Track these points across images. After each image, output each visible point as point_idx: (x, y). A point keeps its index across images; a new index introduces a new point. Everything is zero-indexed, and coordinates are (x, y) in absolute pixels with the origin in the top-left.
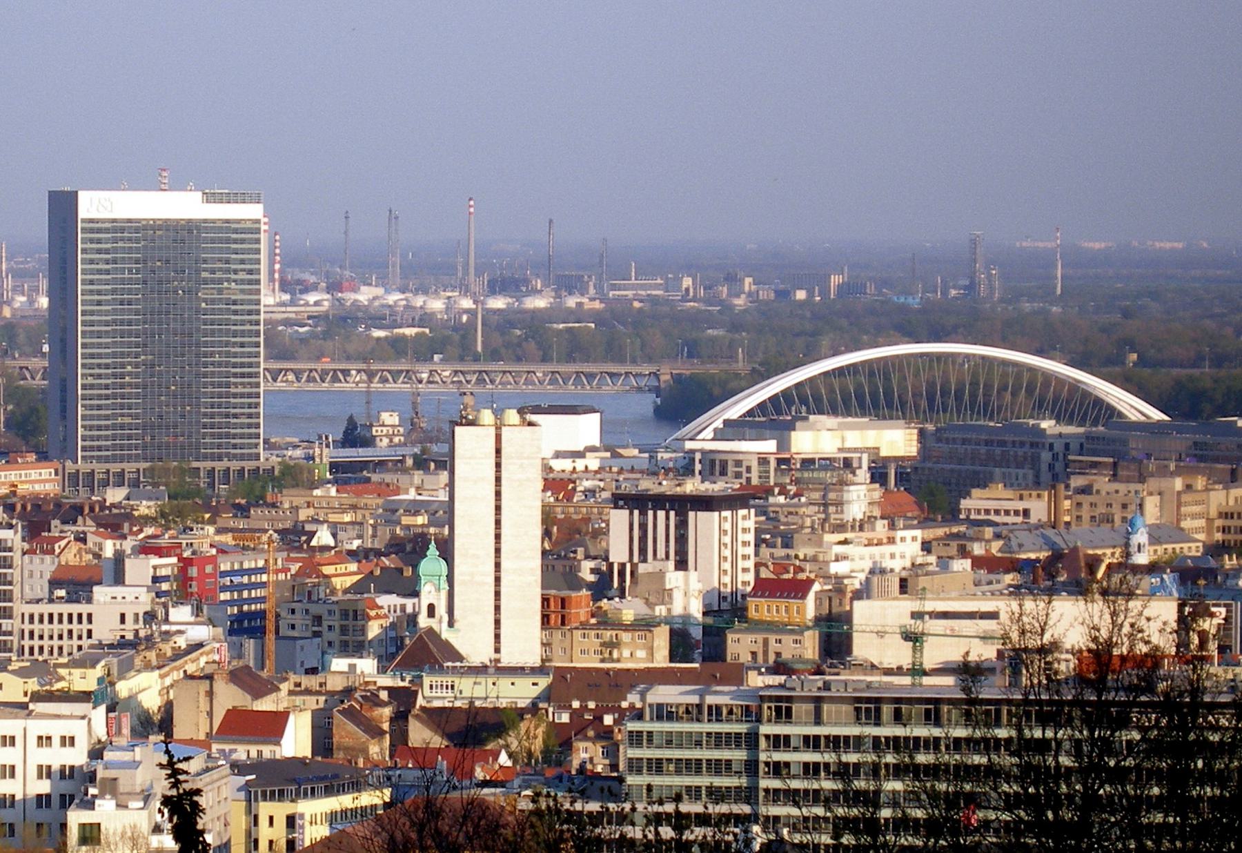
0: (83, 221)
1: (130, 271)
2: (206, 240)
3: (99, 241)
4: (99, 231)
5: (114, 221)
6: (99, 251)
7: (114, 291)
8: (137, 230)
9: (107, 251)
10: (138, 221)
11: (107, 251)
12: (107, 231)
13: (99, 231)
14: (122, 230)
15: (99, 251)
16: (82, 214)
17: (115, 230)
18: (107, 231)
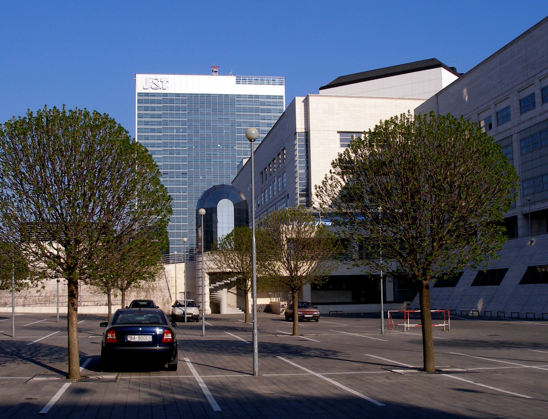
0: (140, 94)
1: (178, 130)
2: (239, 110)
3: (153, 109)
4: (153, 102)
5: (166, 95)
6: (153, 116)
7: (165, 145)
8: (184, 102)
9: (159, 116)
10: (184, 95)
11: (159, 116)
12: (159, 102)
13: (153, 102)
14: (171, 101)
15: (153, 116)
16: (139, 89)
17: (165, 101)
18: (159, 102)
